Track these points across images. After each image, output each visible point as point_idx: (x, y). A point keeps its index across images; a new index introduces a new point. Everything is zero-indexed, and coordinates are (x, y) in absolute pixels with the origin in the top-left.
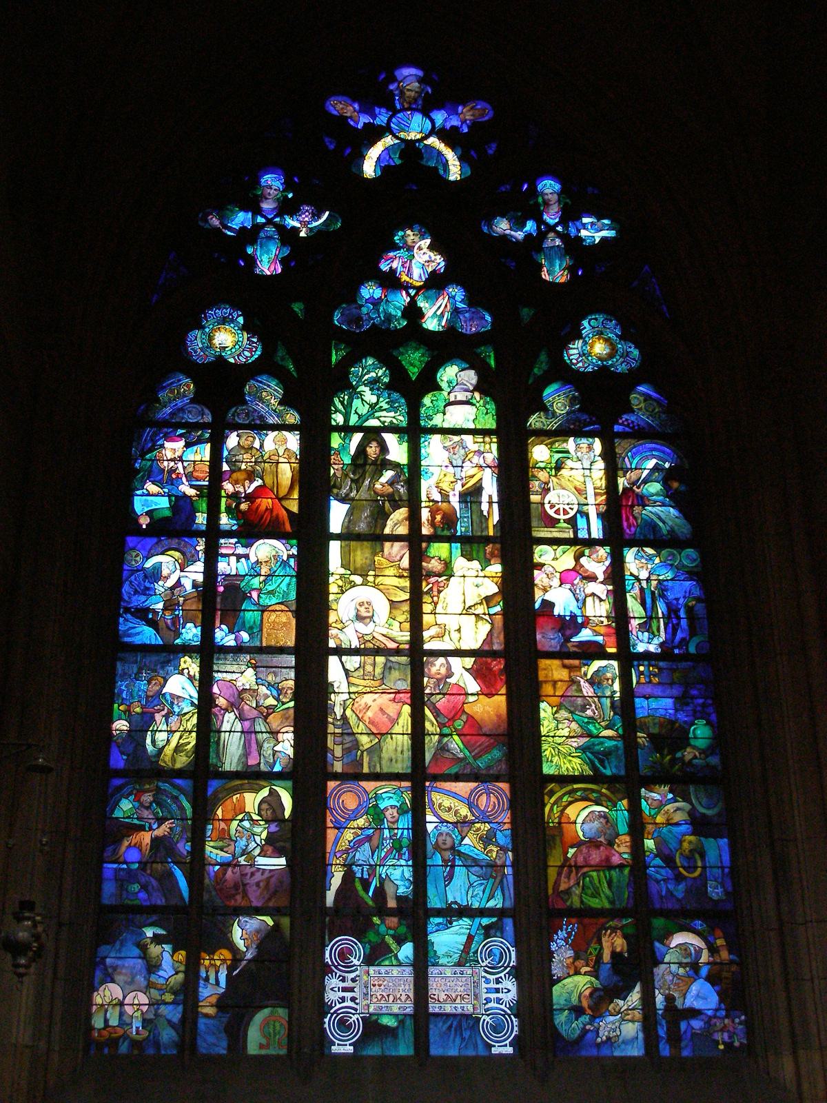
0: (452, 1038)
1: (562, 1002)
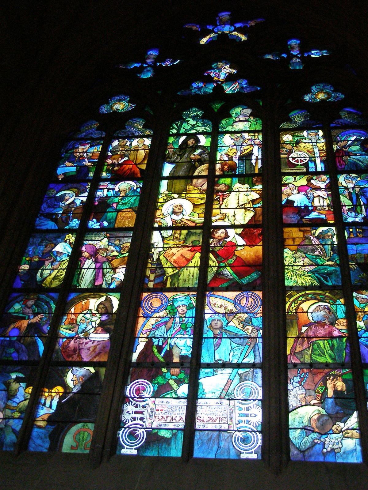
1: (296, 423)
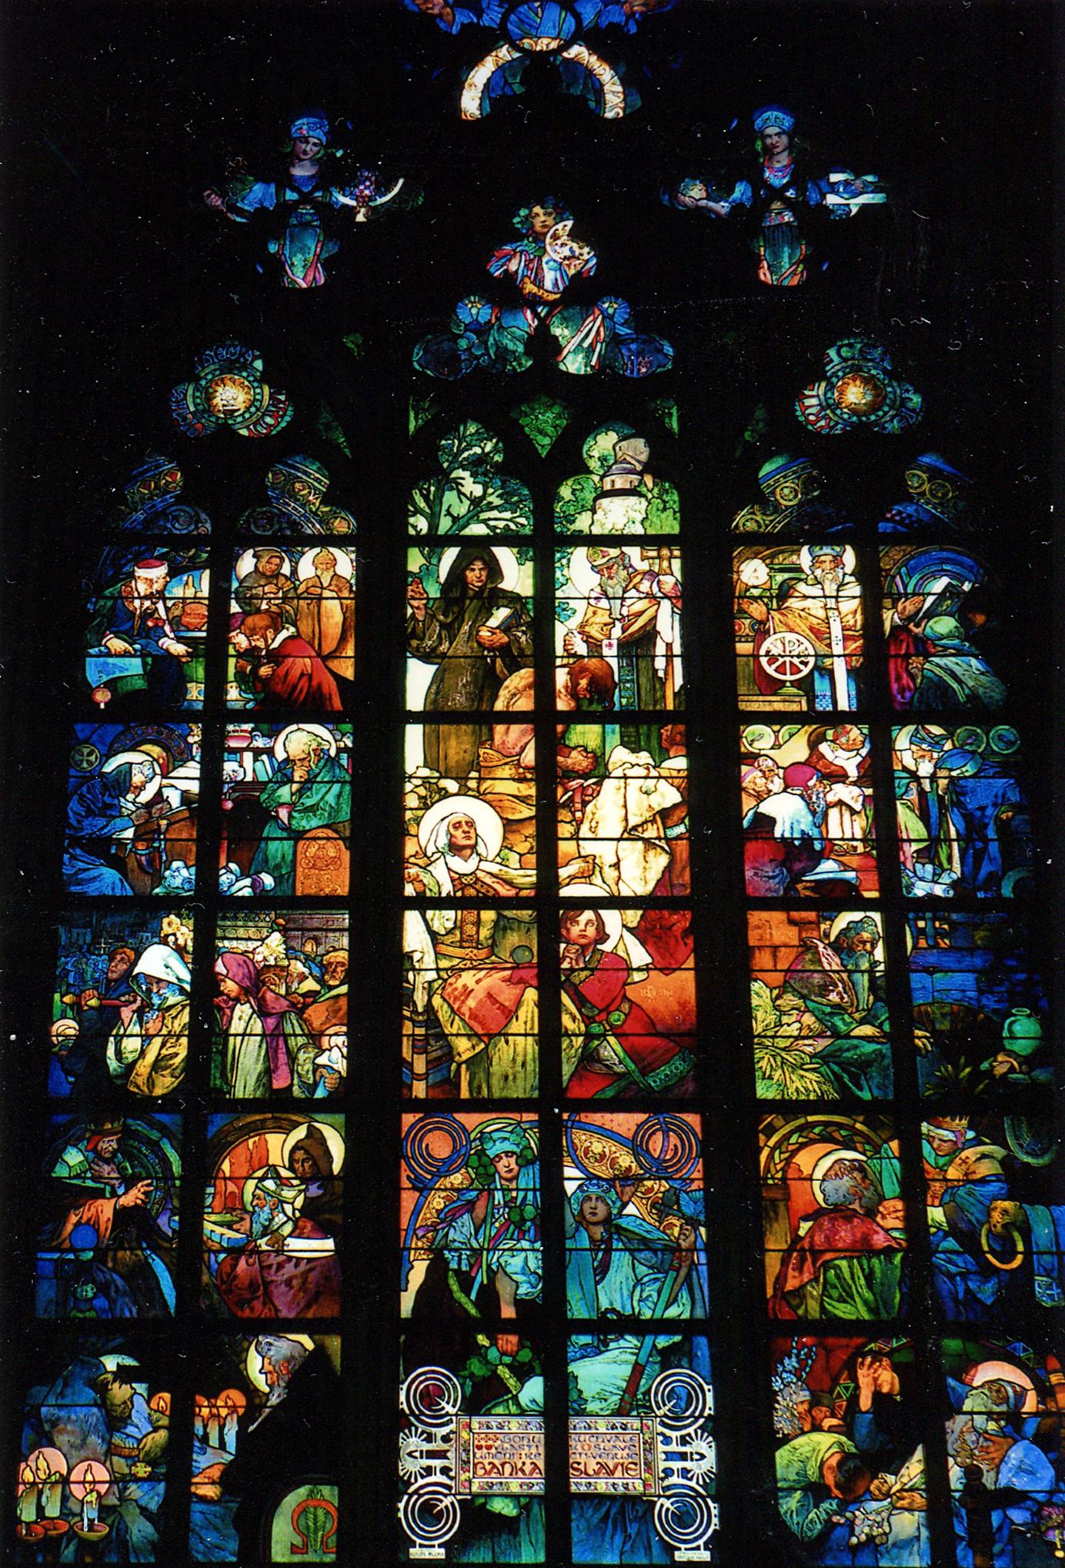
0: (608, 1533)
1: (792, 1477)
